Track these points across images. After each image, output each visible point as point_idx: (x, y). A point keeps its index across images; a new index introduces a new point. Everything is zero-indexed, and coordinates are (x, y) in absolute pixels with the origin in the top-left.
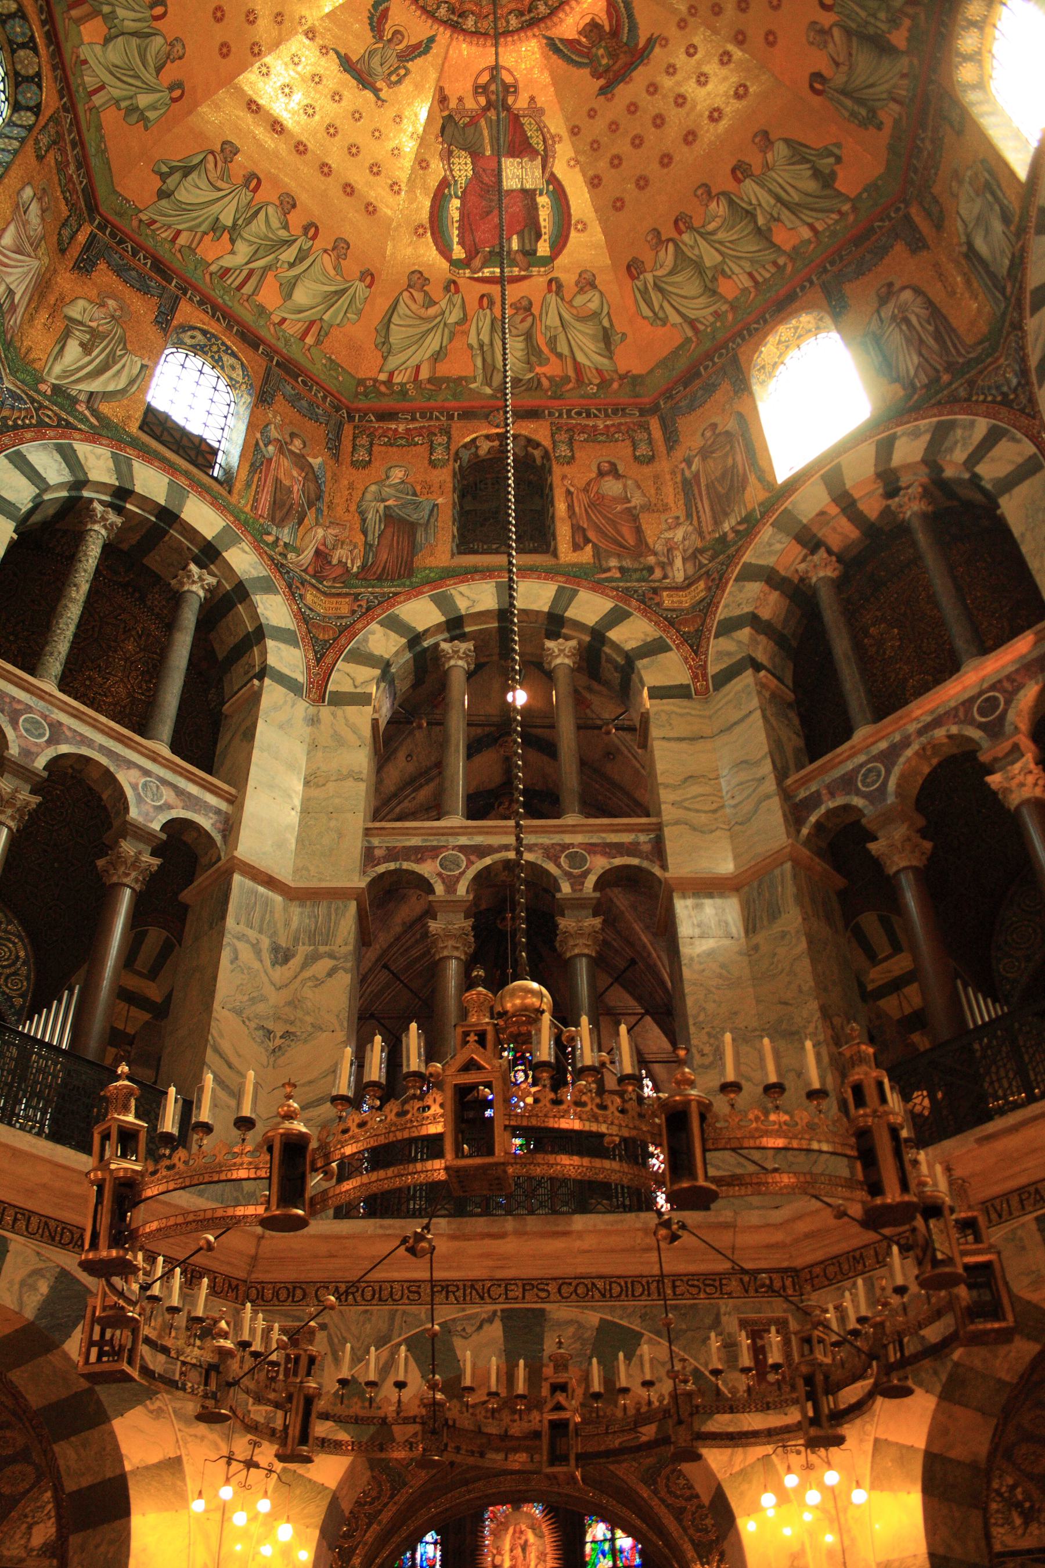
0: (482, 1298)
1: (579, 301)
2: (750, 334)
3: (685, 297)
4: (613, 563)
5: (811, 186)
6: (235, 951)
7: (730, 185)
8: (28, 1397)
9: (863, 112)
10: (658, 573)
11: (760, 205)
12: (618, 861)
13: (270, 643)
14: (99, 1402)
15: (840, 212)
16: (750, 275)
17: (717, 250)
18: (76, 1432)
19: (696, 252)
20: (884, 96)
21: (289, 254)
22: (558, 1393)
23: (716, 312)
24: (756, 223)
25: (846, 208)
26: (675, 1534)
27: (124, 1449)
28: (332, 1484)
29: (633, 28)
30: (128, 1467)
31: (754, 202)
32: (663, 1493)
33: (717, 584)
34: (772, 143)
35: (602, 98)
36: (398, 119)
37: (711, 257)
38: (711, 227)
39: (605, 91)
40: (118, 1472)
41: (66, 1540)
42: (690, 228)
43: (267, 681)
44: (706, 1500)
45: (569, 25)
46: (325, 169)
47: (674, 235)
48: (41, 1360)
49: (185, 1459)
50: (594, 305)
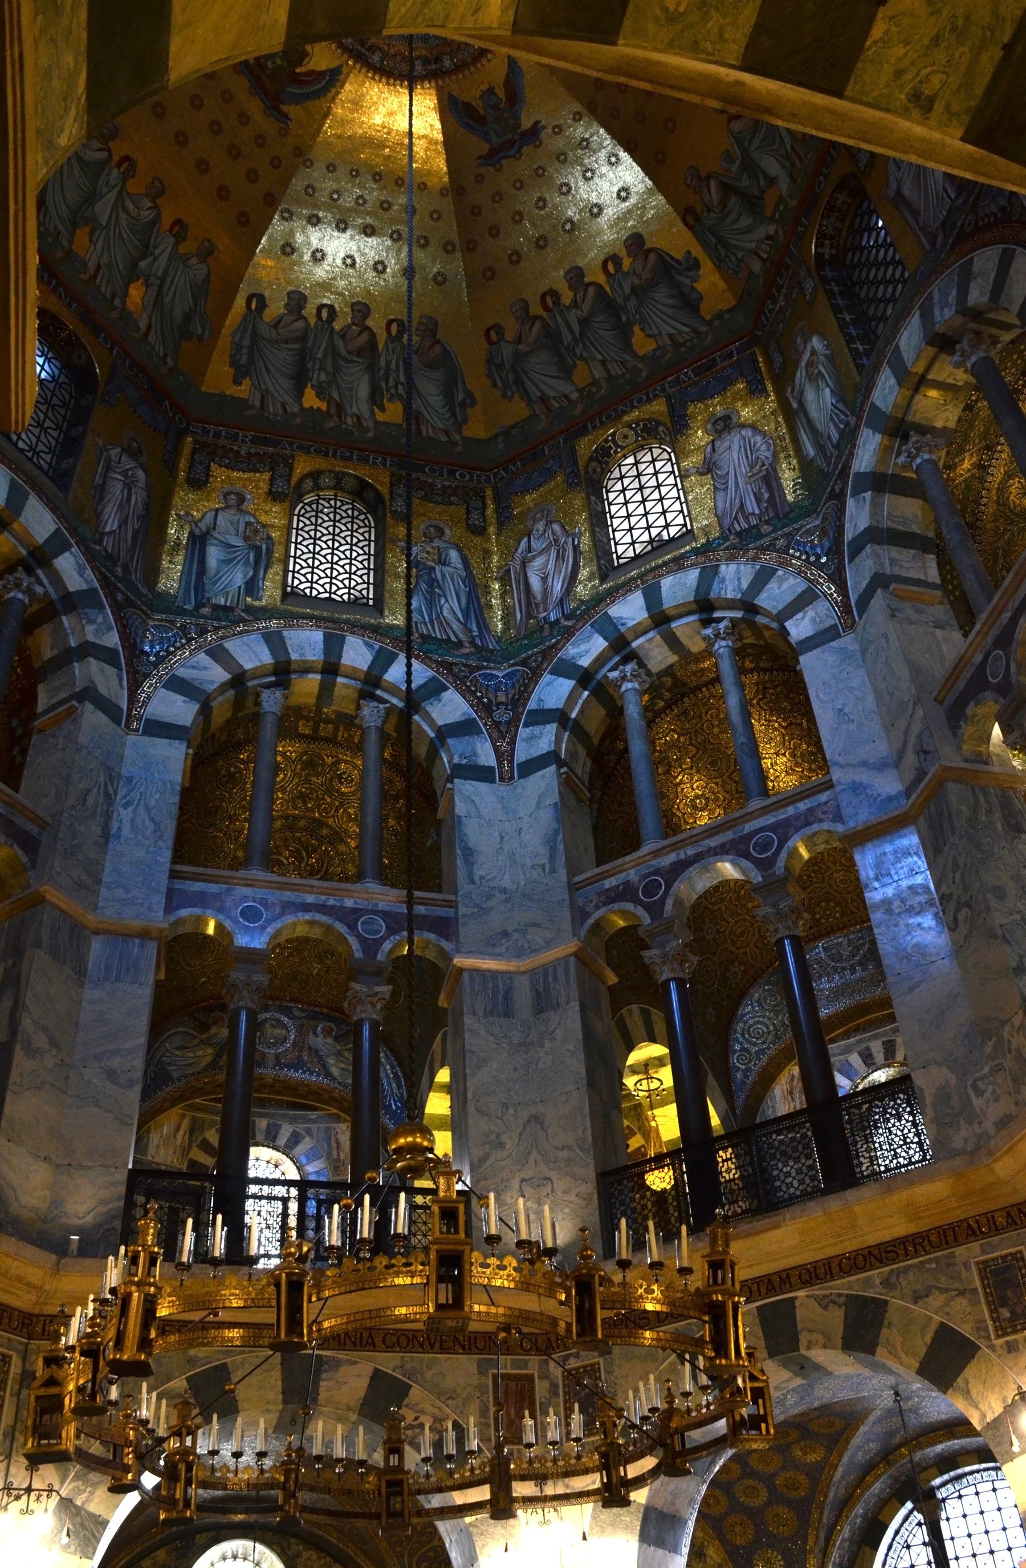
2: (55, 290)
3: (62, 185)
5: (178, 316)
7: (166, 221)
9: (244, 360)
11: (155, 259)
15: (166, 355)
16: (99, 267)
17: (110, 217)
19: (105, 190)
20: (263, 387)
23: (59, 233)
24: (140, 259)
25: (170, 361)
29: (298, 99)
31: (157, 252)
34: (204, 261)
37: (103, 209)
38: (129, 205)
42: (125, 177)
47: (116, 158)
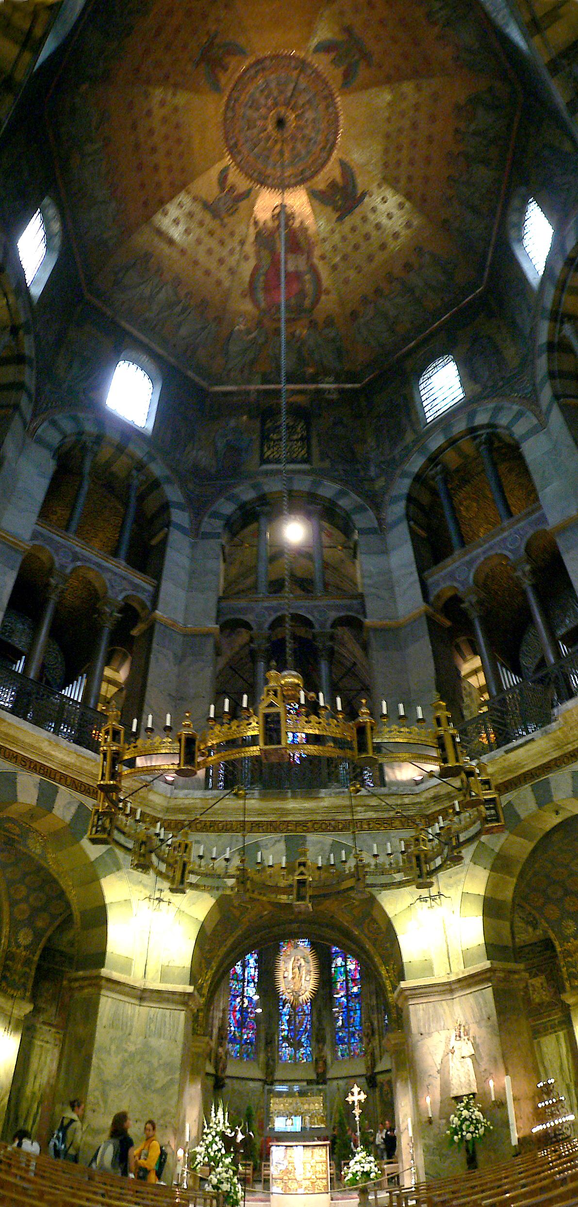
1: (326, 331)
4: (340, 467)
6: (157, 658)
10: (362, 473)
12: (342, 614)
13: (172, 510)
21: (178, 309)
32: (366, 931)
33: (390, 479)
35: (339, 223)
36: (232, 234)
39: (340, 219)
43: (171, 528)
44: (384, 928)
45: (321, 182)
46: (196, 263)
50: (332, 335)
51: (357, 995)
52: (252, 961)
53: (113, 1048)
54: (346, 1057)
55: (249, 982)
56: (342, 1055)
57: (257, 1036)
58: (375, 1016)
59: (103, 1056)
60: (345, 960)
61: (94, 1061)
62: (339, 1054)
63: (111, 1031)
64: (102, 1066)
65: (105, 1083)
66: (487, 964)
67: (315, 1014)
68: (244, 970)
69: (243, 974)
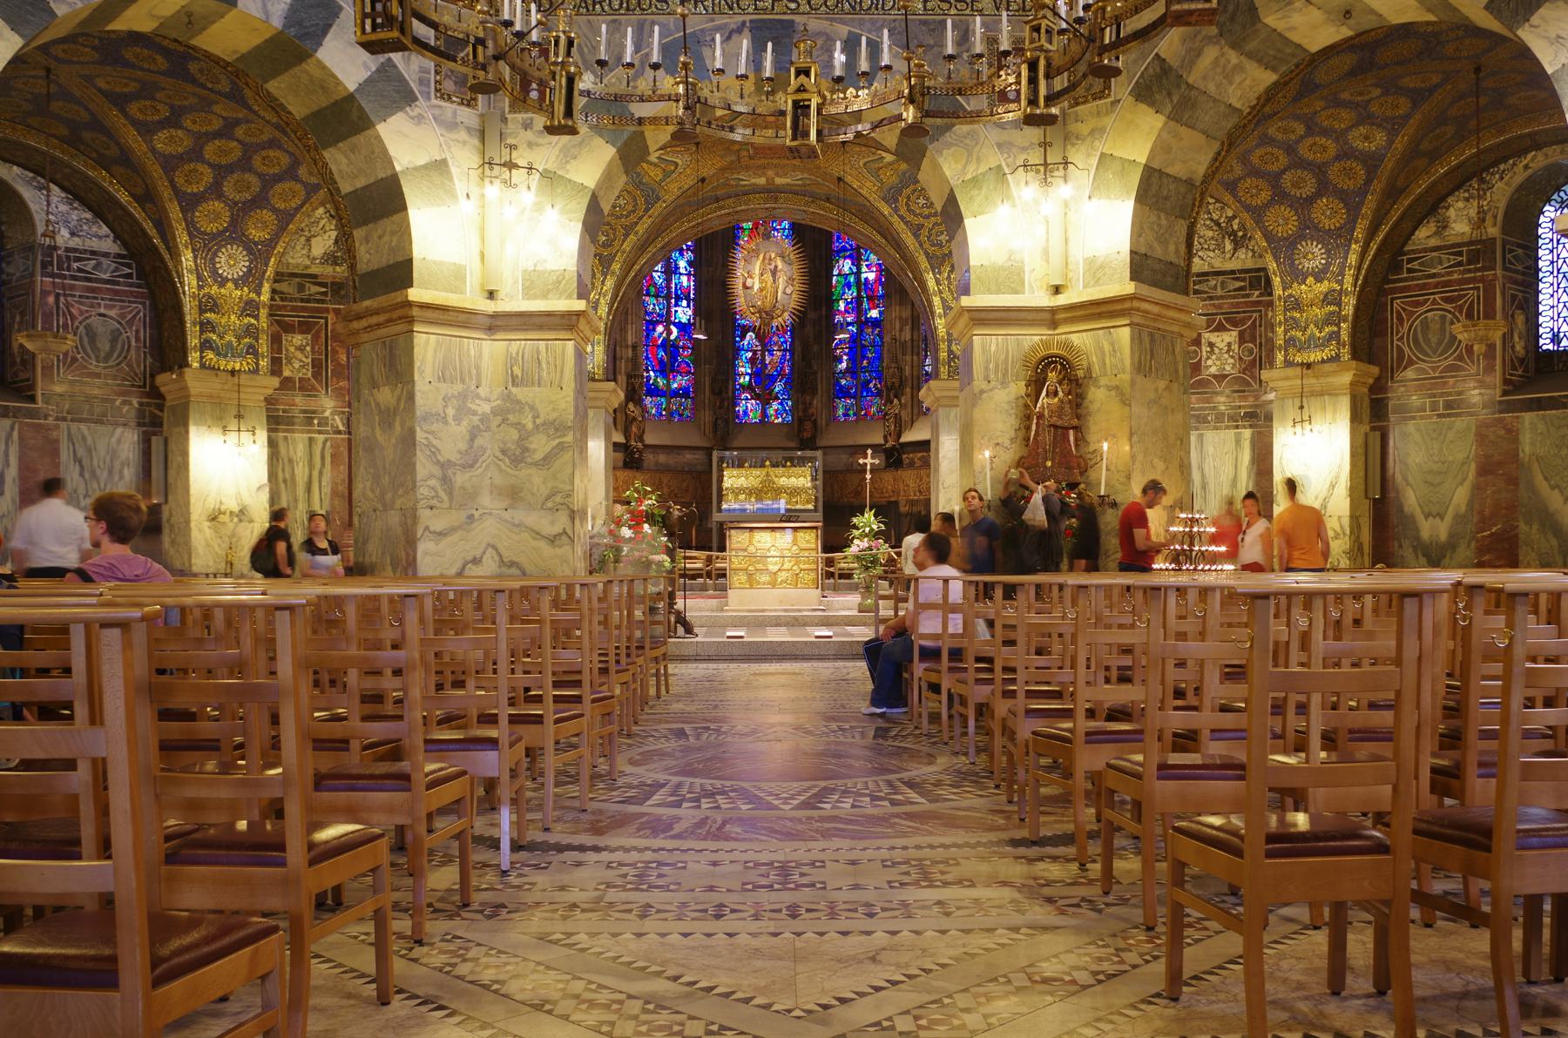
0: (731, 8)
8: (290, 108)
14: (361, 109)
18: (343, 138)
22: (802, 77)
26: (911, 248)
27: (392, 151)
28: (591, 183)
30: (398, 168)
40: (389, 173)
41: (351, 235)
48: (296, 70)
49: (450, 162)
51: (876, 323)
52: (682, 264)
53: (451, 412)
54: (852, 418)
55: (678, 299)
56: (846, 415)
57: (697, 383)
58: (908, 358)
59: (435, 427)
60: (857, 261)
61: (420, 436)
62: (840, 412)
63: (443, 386)
64: (435, 442)
65: (445, 466)
66: (1129, 288)
67: (798, 349)
68: (668, 280)
69: (669, 288)
